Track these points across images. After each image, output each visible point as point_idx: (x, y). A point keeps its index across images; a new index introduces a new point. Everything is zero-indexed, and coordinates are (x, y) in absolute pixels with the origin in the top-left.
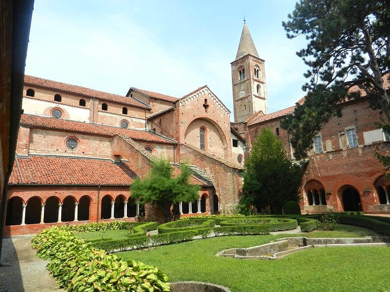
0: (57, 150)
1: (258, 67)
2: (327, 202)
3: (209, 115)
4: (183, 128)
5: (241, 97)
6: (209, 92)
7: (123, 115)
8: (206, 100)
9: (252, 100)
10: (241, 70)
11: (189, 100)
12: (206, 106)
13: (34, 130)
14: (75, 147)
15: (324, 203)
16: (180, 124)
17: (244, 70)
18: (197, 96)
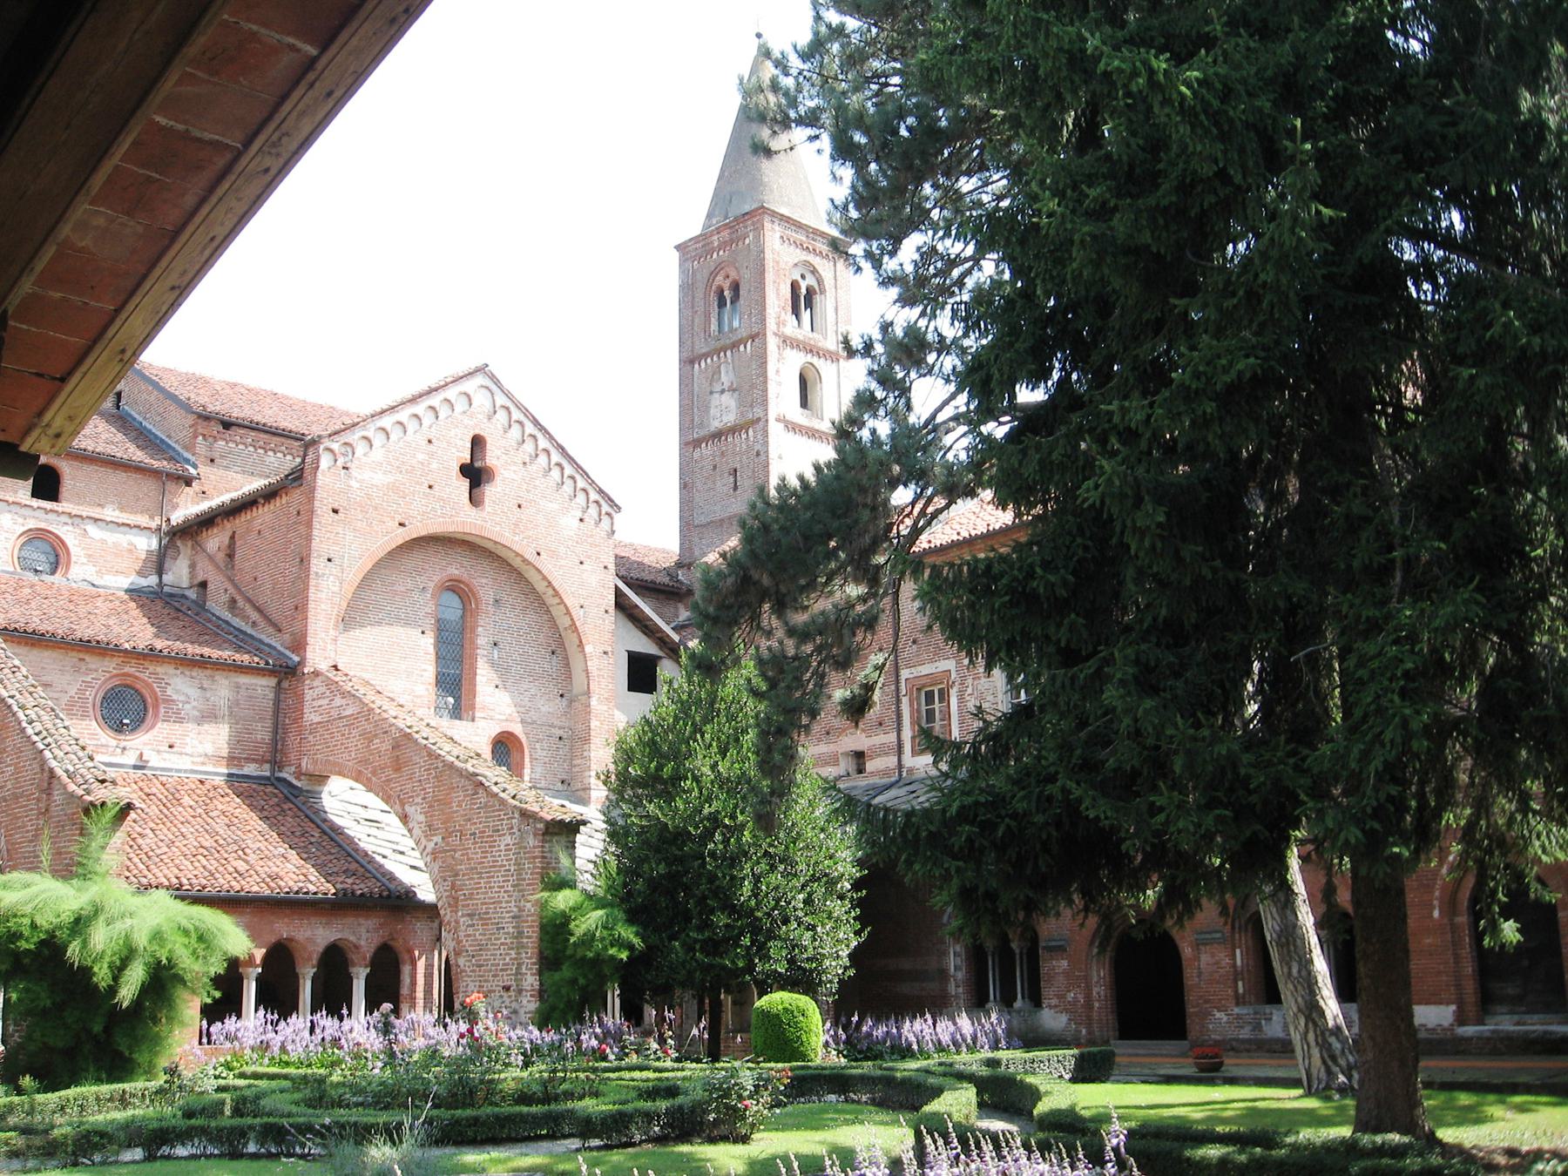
1: (814, 272)
2: (1049, 994)
3: (490, 519)
4: (328, 591)
5: (716, 425)
6: (501, 400)
7: (36, 503)
8: (477, 443)
9: (766, 443)
10: (726, 285)
11: (378, 440)
12: (475, 475)
15: (1036, 1000)
16: (317, 564)
17: (736, 287)
18: (428, 419)
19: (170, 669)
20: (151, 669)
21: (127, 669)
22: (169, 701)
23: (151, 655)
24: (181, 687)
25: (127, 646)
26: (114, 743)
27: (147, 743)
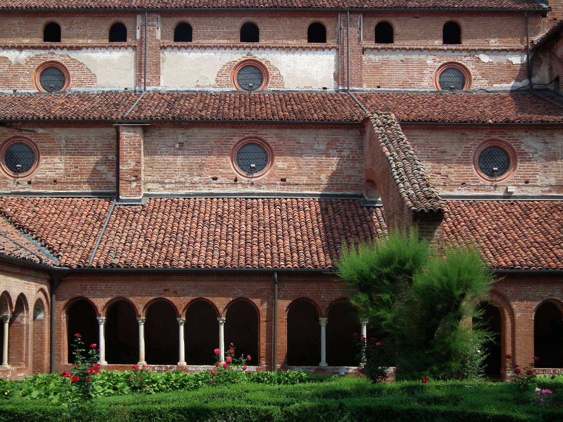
0: (215, 179)
13: (156, 132)
14: (260, 167)
19: (523, 134)
20: (509, 134)
21: (493, 137)
22: (523, 153)
23: (507, 126)
24: (530, 143)
25: (490, 121)
26: (489, 183)
27: (511, 183)
